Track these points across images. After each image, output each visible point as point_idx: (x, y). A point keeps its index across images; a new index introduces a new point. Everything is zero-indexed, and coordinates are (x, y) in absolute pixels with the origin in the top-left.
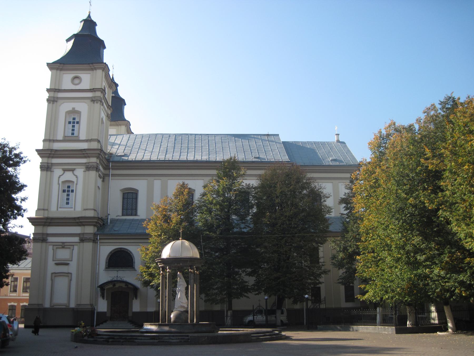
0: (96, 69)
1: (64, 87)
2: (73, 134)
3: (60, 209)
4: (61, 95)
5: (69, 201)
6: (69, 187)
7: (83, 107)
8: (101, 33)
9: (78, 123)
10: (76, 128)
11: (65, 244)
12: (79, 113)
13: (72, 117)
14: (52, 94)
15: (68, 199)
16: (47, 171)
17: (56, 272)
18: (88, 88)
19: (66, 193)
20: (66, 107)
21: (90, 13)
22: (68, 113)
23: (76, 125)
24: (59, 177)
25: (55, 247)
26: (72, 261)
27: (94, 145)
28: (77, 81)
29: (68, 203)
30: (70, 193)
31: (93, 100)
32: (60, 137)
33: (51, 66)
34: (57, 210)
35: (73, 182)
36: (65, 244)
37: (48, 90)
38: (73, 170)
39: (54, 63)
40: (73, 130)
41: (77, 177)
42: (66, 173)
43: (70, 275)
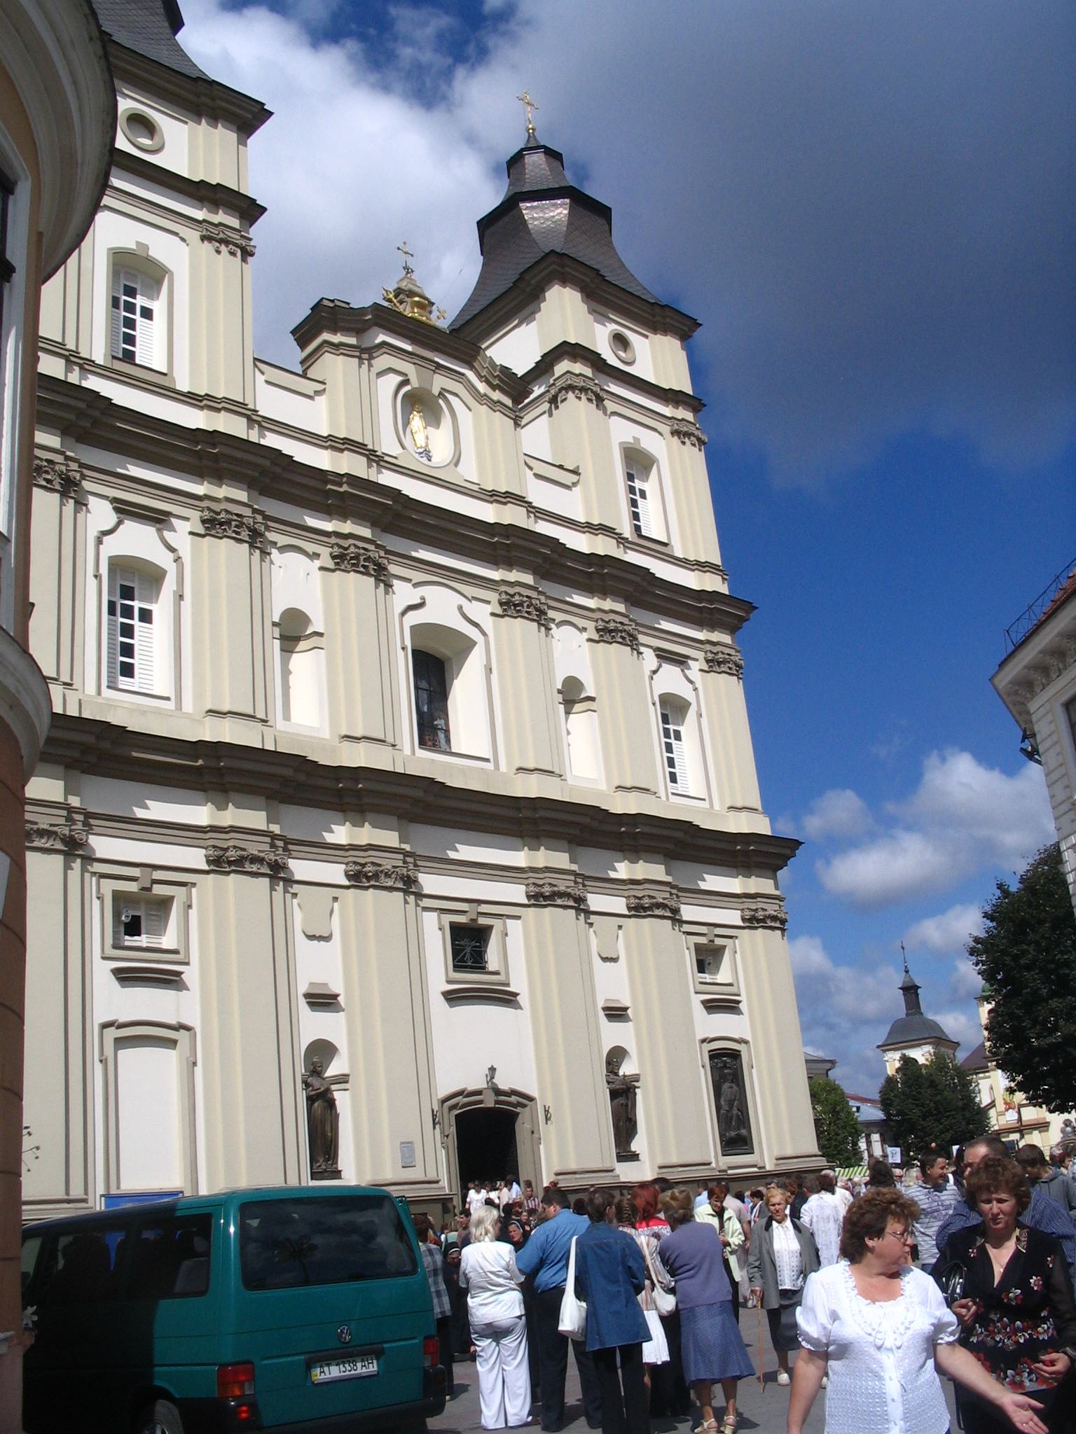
2: (129, 357)
3: (106, 692)
5: (136, 661)
9: (147, 313)
11: (158, 875)
13: (123, 282)
15: (128, 650)
17: (122, 1019)
24: (99, 542)
25: (109, 886)
26: (187, 964)
29: (128, 670)
30: (136, 622)
34: (99, 693)
35: (151, 577)
36: (158, 875)
38: (159, 519)
40: (130, 340)
41: (178, 559)
42: (130, 526)
43: (181, 1036)
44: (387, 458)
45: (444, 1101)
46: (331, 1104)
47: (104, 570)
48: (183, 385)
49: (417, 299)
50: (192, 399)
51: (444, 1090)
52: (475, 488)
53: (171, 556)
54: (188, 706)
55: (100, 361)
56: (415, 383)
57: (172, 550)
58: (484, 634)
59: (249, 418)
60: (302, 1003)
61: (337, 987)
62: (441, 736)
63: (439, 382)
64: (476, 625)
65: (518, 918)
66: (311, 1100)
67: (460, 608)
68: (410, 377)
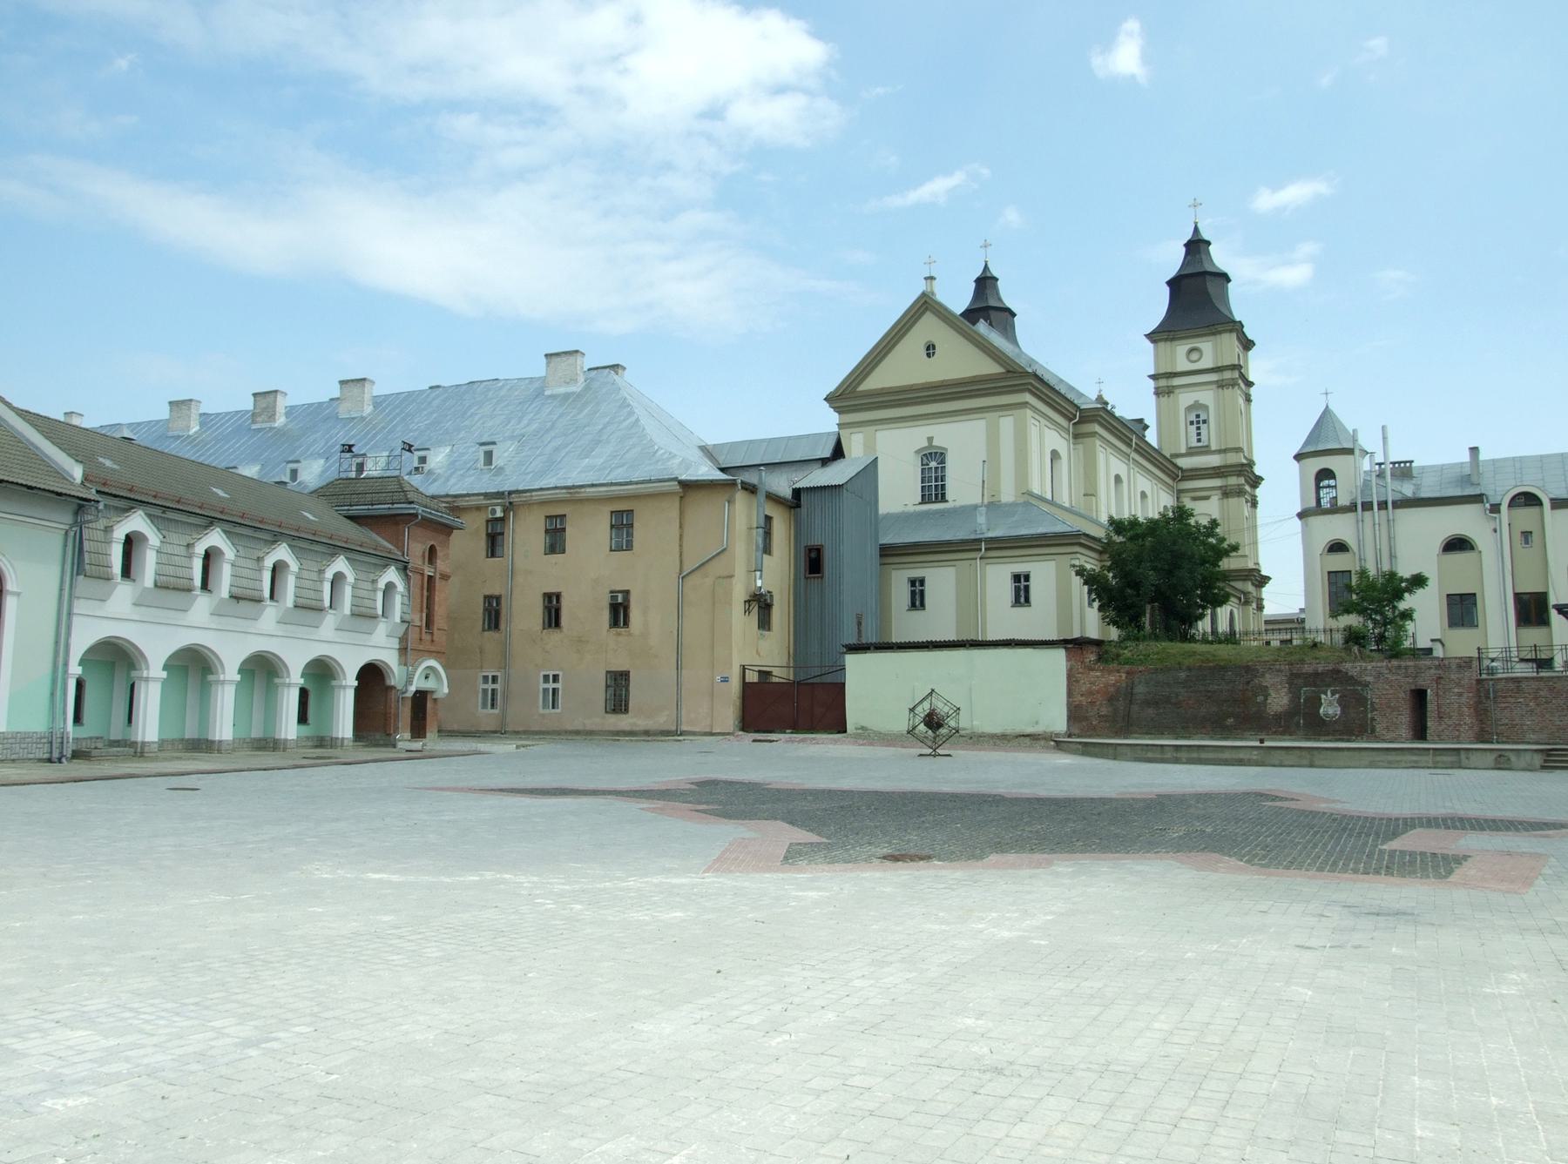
0: (1220, 333)
1: (1179, 369)
4: (1177, 381)
7: (1207, 397)
8: (1220, 257)
10: (1204, 431)
12: (1206, 408)
14: (1163, 382)
18: (1210, 365)
20: (1185, 399)
21: (1196, 230)
27: (1232, 459)
28: (1194, 356)
31: (1221, 385)
32: (1183, 450)
33: (1153, 337)
37: (1154, 377)
39: (1153, 332)
55: (1183, 450)
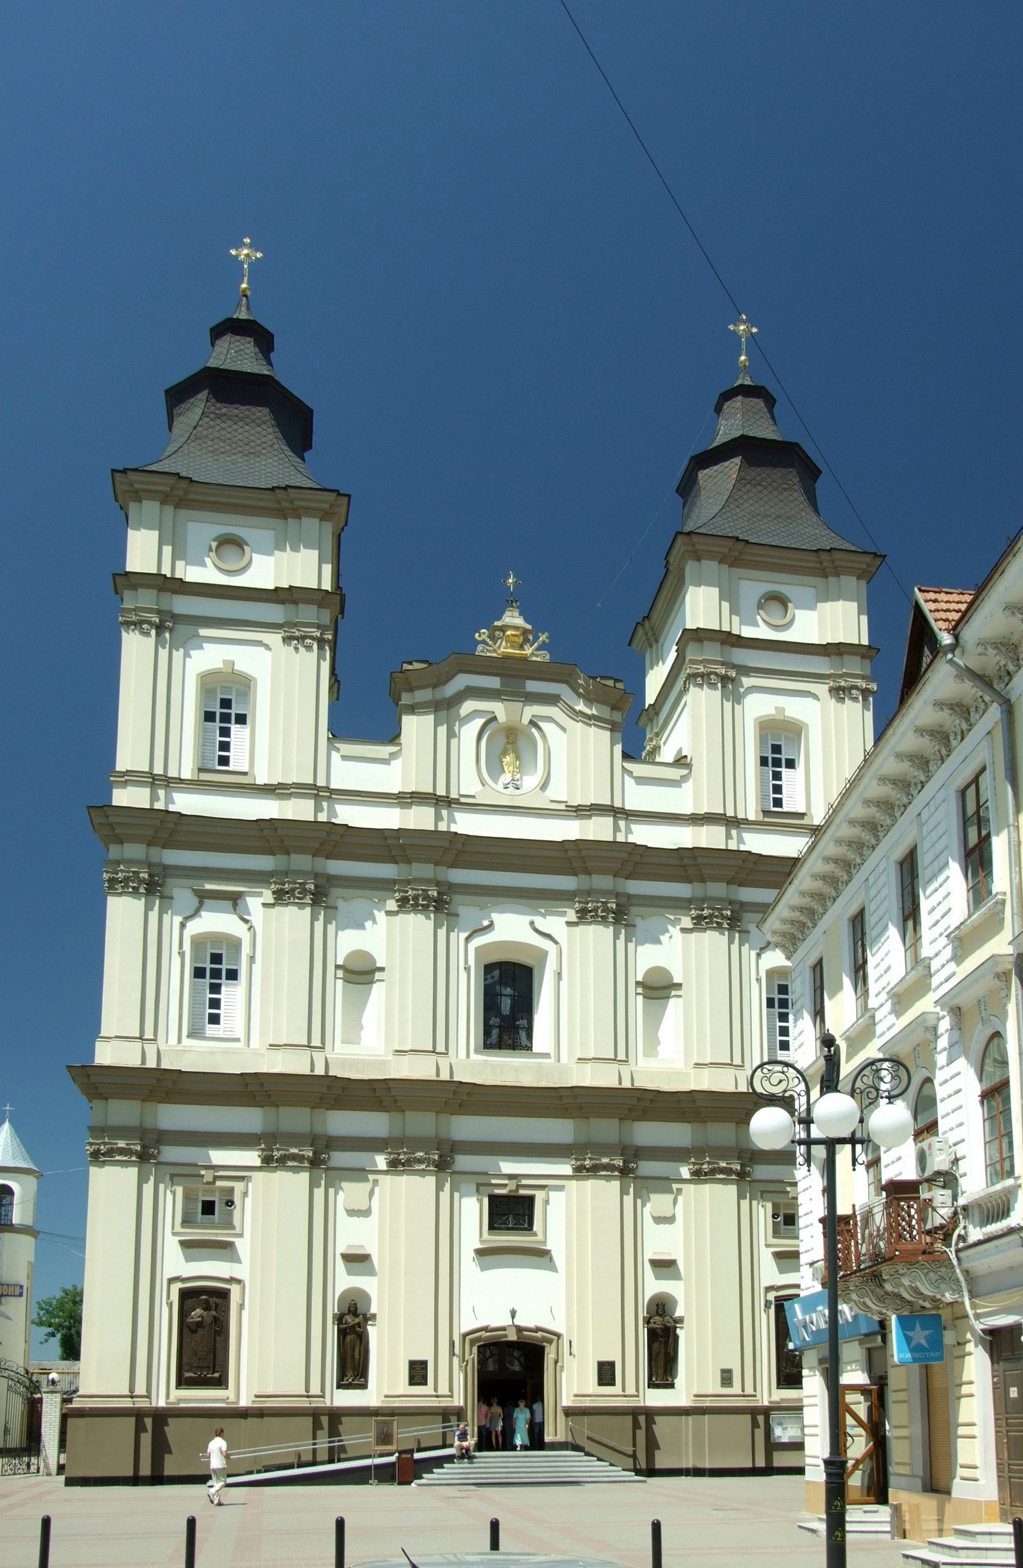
2: (224, 761)
5: (222, 1012)
6: (216, 958)
16: (149, 892)
19: (208, 981)
22: (208, 682)
23: (235, 728)
29: (214, 1019)
34: (179, 1041)
40: (225, 746)
44: (463, 800)
45: (465, 1336)
46: (362, 1338)
47: (187, 947)
48: (261, 780)
49: (509, 633)
50: (270, 790)
51: (466, 1328)
52: (562, 807)
53: (246, 926)
54: (255, 1043)
56: (502, 718)
57: (246, 921)
58: (556, 942)
59: (316, 796)
60: (339, 1260)
61: (371, 1248)
62: (523, 1034)
63: (531, 711)
64: (548, 936)
65: (561, 1188)
66: (342, 1333)
67: (532, 923)
68: (496, 714)
